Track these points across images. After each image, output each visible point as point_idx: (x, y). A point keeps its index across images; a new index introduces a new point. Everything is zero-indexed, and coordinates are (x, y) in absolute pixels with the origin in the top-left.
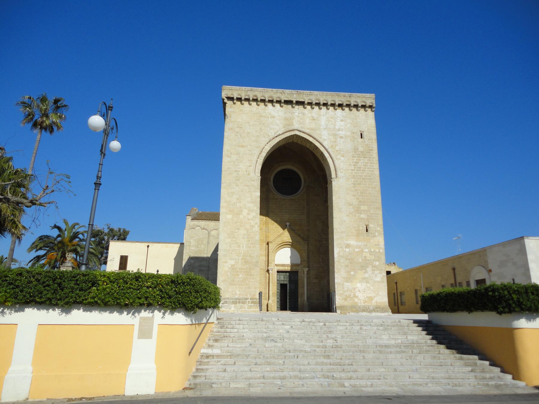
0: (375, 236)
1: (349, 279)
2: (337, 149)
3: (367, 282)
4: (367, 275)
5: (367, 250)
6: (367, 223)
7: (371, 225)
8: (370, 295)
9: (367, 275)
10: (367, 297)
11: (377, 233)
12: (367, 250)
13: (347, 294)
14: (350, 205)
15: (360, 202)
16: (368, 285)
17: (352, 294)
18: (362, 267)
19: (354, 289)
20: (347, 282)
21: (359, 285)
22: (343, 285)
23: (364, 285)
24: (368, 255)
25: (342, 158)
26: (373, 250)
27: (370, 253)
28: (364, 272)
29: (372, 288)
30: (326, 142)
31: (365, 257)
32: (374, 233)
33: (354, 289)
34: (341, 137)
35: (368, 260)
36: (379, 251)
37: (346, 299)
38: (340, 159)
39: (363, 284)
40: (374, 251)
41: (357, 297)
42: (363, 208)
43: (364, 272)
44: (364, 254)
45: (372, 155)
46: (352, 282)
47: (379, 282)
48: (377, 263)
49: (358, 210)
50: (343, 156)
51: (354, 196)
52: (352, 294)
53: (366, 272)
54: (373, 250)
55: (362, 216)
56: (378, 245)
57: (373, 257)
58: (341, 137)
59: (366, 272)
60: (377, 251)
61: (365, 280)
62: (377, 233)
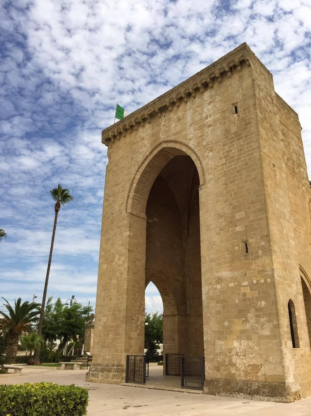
0: (258, 257)
1: (223, 334)
2: (204, 144)
3: (249, 338)
4: (248, 326)
5: (246, 283)
6: (244, 238)
7: (250, 241)
8: (254, 362)
9: (248, 326)
10: (249, 365)
11: (260, 252)
12: (246, 283)
13: (220, 359)
14: (221, 217)
15: (234, 208)
16: (251, 344)
17: (227, 360)
18: (240, 311)
19: (230, 350)
20: (219, 339)
21: (236, 344)
22: (214, 344)
23: (244, 343)
24: (248, 290)
25: (211, 153)
26: (255, 282)
27: (252, 286)
28: (244, 321)
29: (256, 348)
30: (192, 142)
31: (245, 294)
32: (257, 252)
33: (230, 350)
34: (209, 126)
35: (249, 300)
36: (265, 280)
37: (218, 369)
38: (208, 156)
39: (243, 342)
40: (257, 283)
41: (234, 365)
42: (238, 216)
43: (244, 321)
44: (243, 290)
45: (250, 131)
46: (226, 339)
47: (267, 337)
48: (263, 303)
49: (232, 223)
50: (211, 151)
51: (225, 202)
52: (227, 360)
53: (246, 321)
54: (255, 282)
55: (238, 229)
56: (264, 271)
57: (256, 294)
58: (209, 126)
59: (246, 321)
60: (263, 281)
61: (245, 335)
62: (260, 252)
